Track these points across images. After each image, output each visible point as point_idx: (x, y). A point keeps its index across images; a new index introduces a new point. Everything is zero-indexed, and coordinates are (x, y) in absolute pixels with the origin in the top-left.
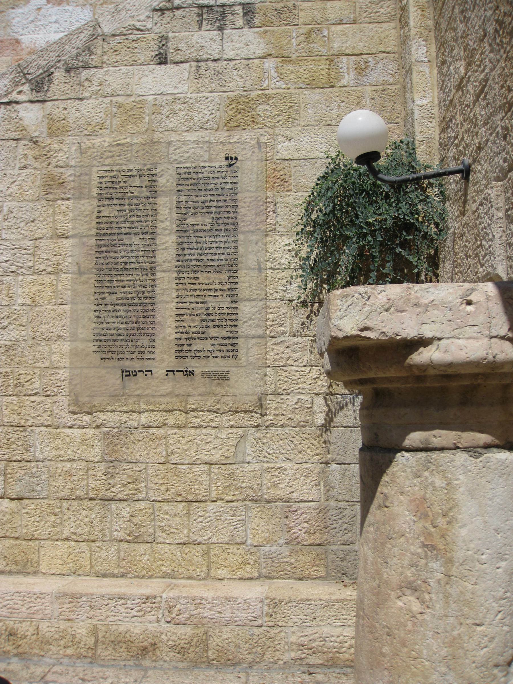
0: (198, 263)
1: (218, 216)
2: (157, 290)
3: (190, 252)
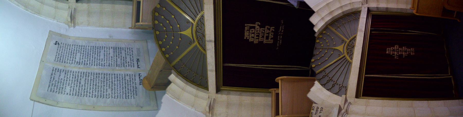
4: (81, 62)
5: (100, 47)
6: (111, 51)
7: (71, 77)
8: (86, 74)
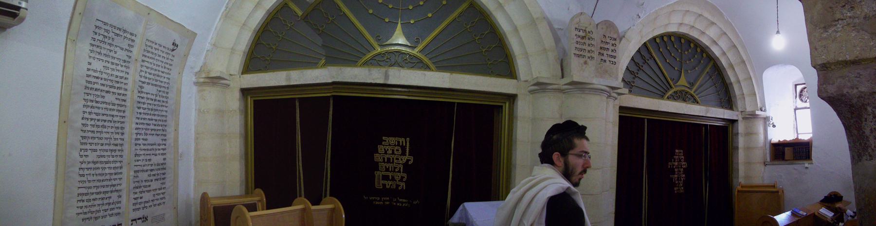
4: (142, 95)
5: (165, 135)
6: (159, 159)
8: (121, 106)
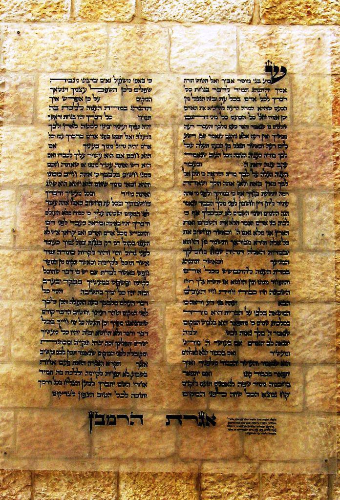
0: (220, 237)
1: (254, 161)
2: (152, 280)
3: (207, 217)
7: (119, 152)
